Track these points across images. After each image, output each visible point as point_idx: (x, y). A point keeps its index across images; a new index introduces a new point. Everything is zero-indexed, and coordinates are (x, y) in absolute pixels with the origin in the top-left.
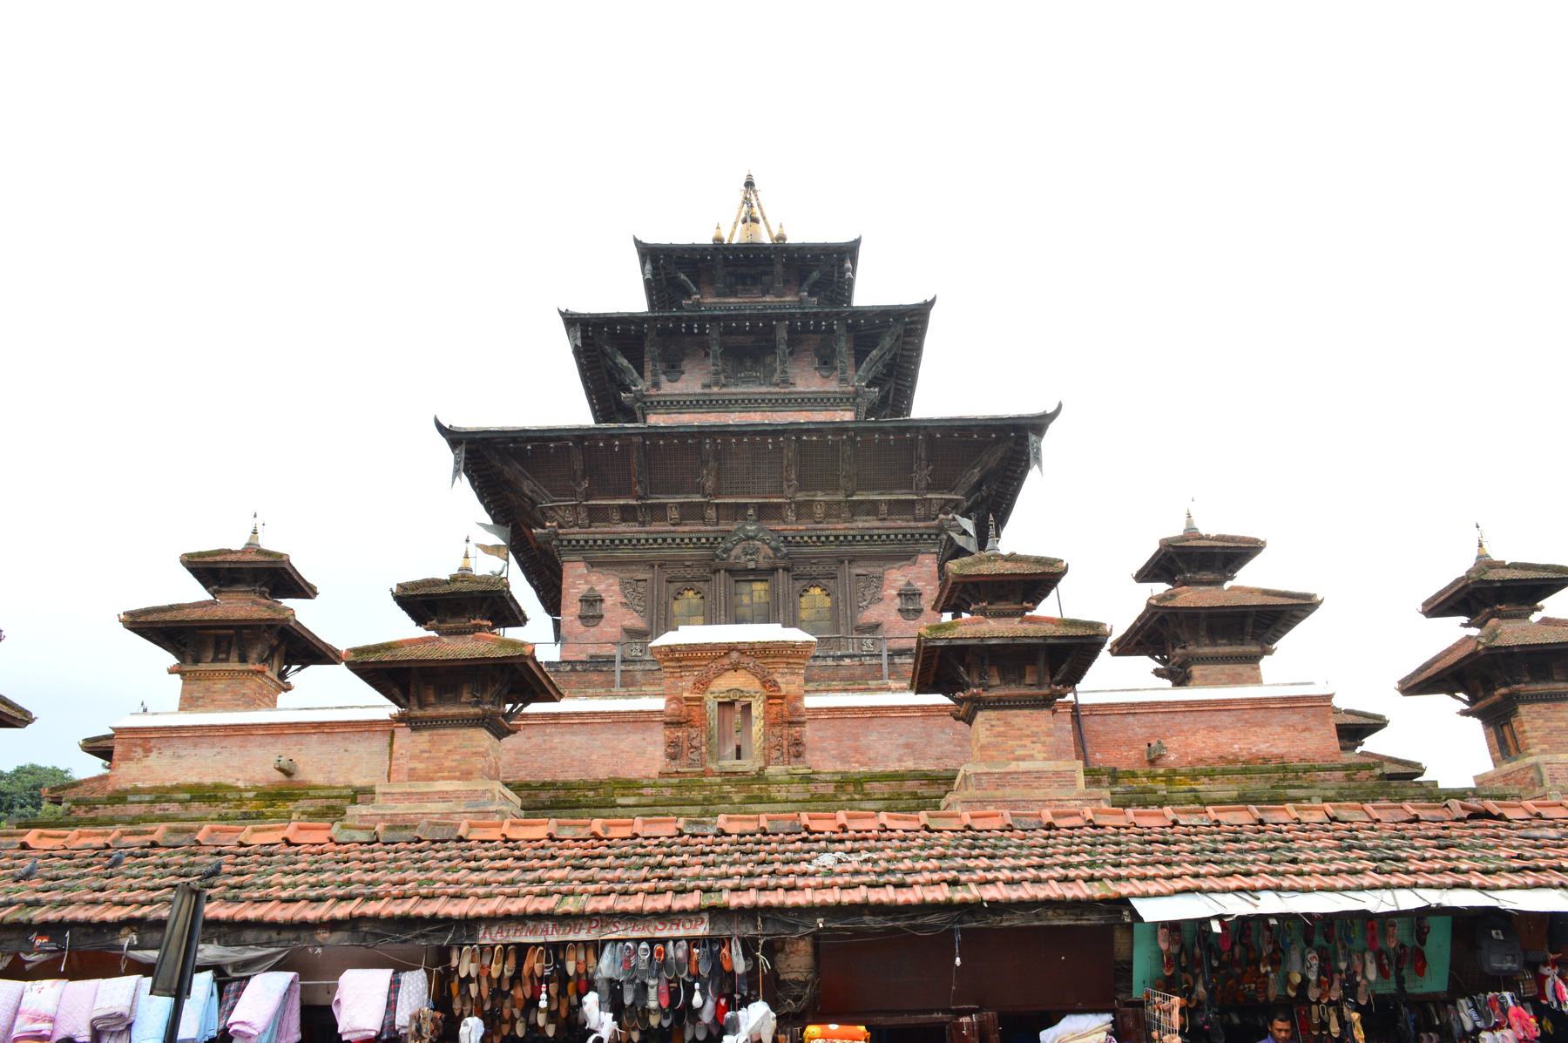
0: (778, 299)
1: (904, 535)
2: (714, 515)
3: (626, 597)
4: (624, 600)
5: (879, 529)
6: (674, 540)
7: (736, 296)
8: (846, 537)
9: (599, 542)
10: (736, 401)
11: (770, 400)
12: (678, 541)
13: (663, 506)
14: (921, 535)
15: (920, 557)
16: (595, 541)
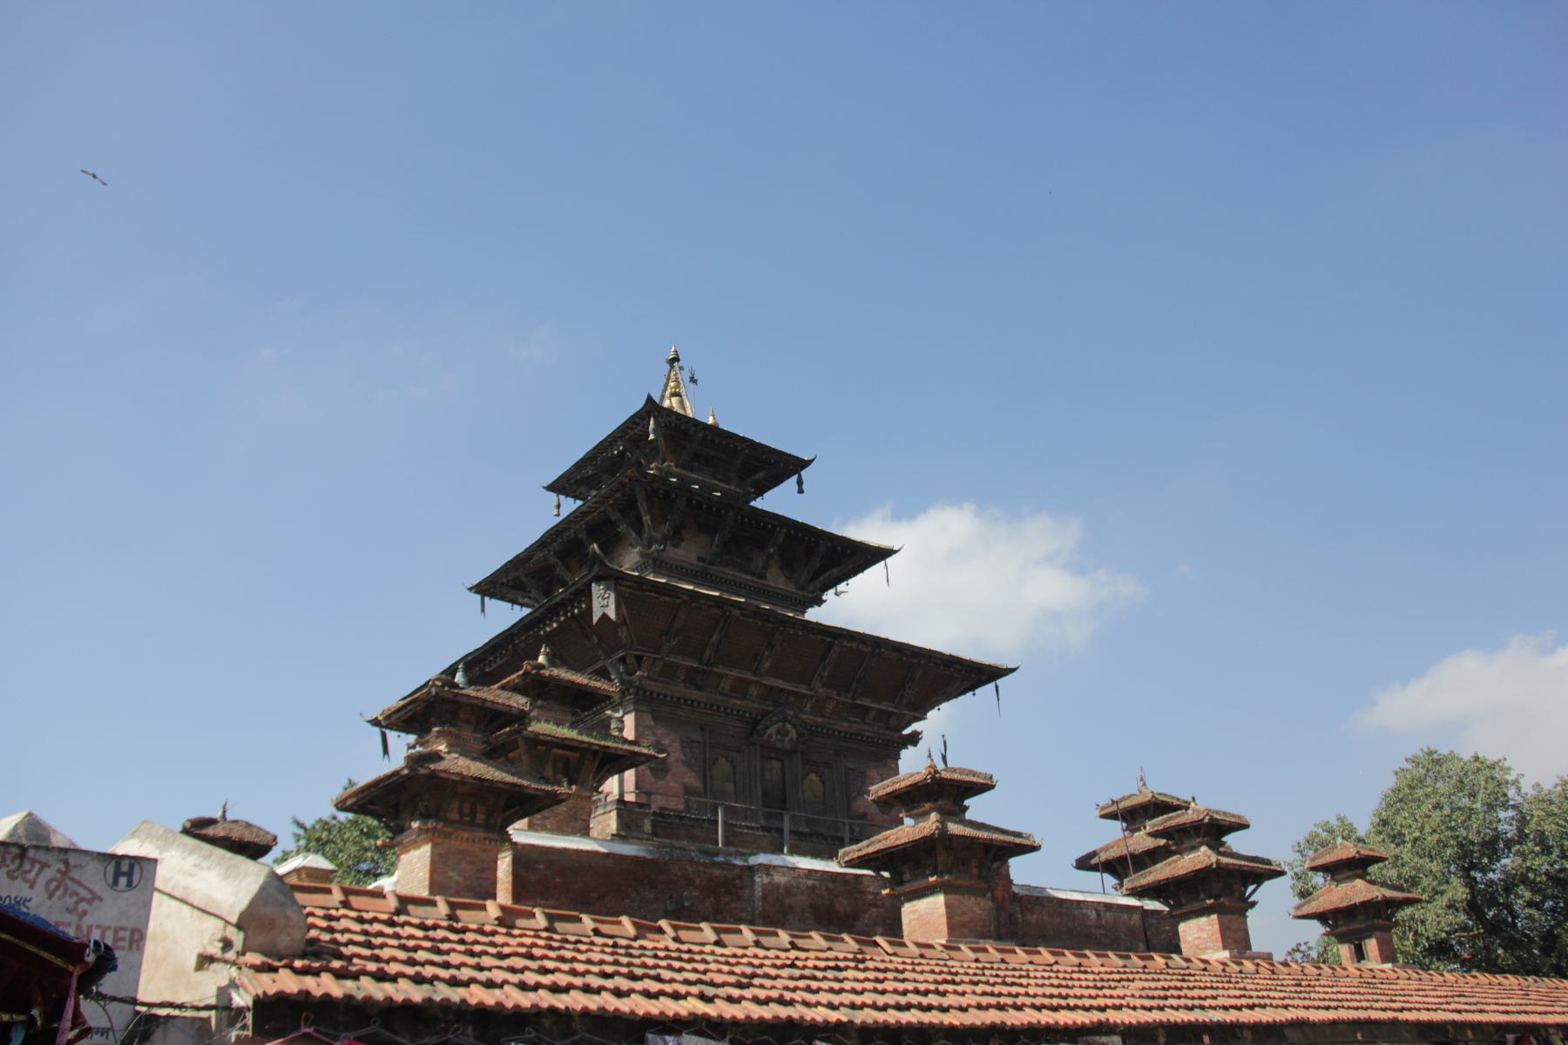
0: (727, 487)
1: (883, 741)
2: (755, 693)
3: (685, 756)
4: (684, 758)
5: (869, 731)
6: (726, 708)
7: (692, 471)
8: (846, 733)
9: (668, 698)
10: (726, 580)
11: (750, 587)
12: (729, 711)
13: (721, 676)
14: (893, 742)
15: (889, 760)
16: (665, 696)
